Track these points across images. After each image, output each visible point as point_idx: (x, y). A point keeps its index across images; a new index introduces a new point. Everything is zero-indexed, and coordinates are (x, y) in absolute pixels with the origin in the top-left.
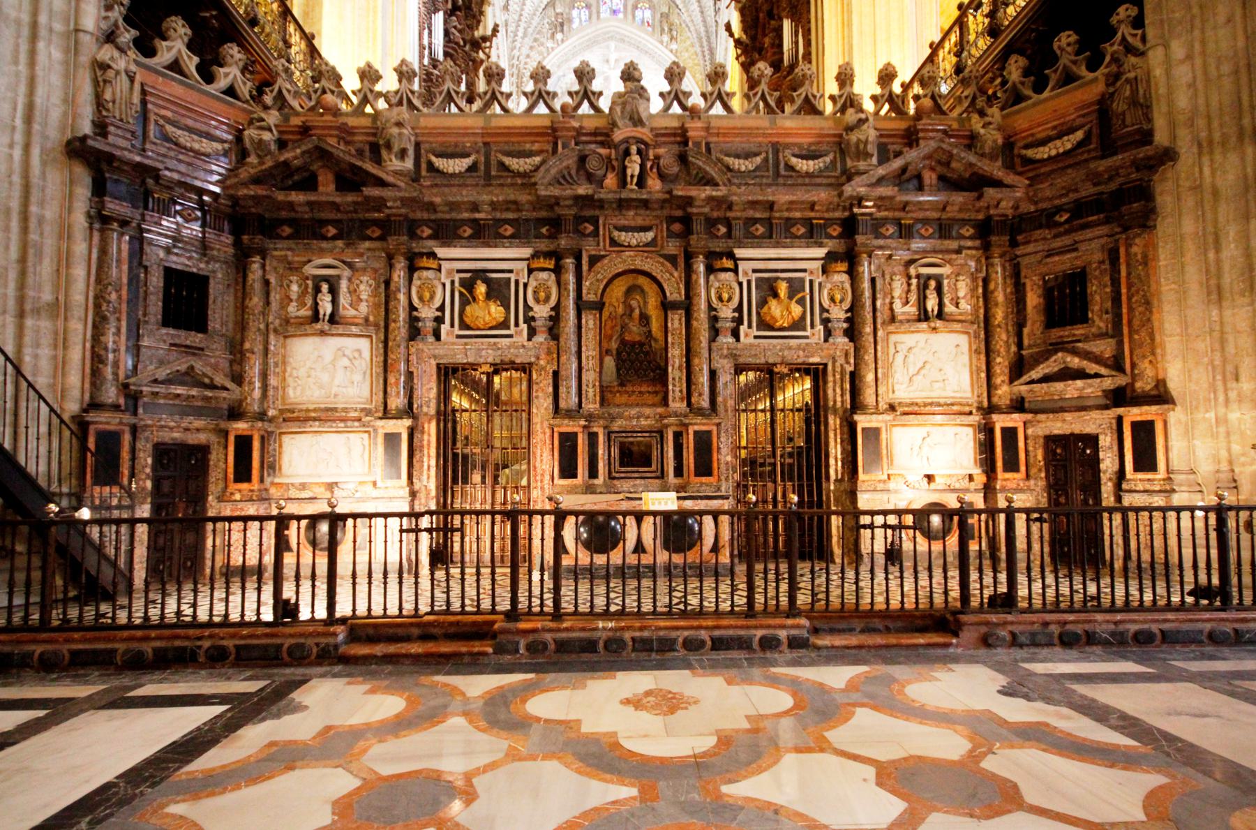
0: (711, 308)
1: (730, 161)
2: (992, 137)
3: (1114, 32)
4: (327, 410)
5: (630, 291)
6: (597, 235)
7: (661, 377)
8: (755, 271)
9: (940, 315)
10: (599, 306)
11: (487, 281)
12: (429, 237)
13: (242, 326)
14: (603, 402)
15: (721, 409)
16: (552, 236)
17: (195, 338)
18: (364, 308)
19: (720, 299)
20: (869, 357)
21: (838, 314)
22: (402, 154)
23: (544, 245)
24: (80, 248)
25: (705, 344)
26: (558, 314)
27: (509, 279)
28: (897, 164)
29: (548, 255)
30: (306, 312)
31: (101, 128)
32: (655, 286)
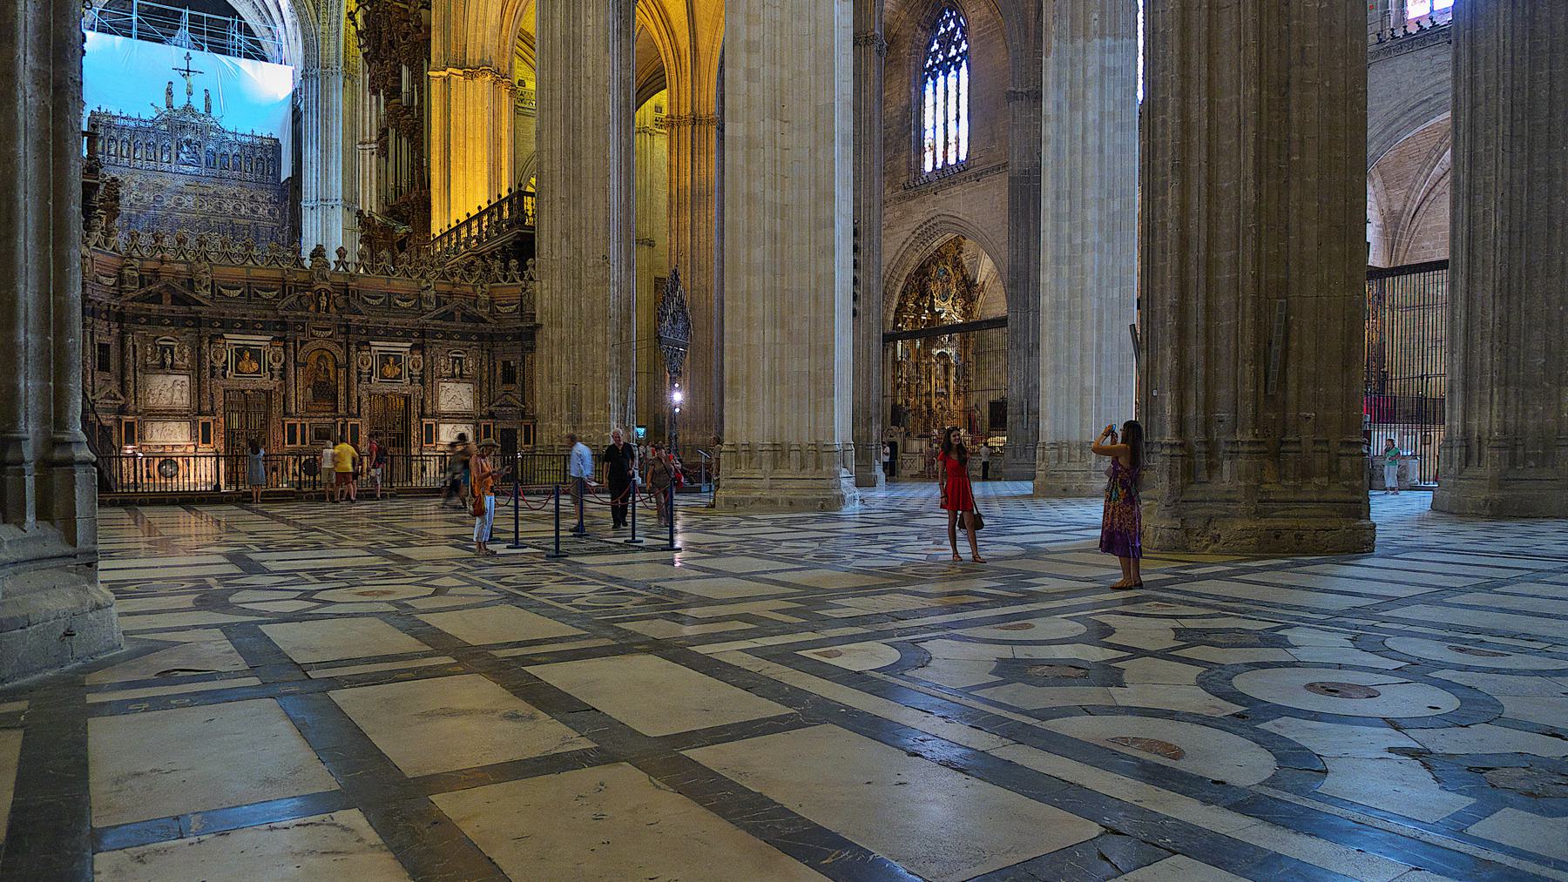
3: (526, 269)
4: (171, 411)
6: (304, 331)
8: (379, 351)
11: (249, 350)
12: (219, 327)
15: (362, 414)
16: (285, 330)
18: (186, 361)
19: (362, 363)
21: (416, 372)
22: (206, 287)
23: (277, 334)
25: (355, 385)
26: (285, 368)
27: (260, 350)
29: (280, 339)
32: (332, 357)
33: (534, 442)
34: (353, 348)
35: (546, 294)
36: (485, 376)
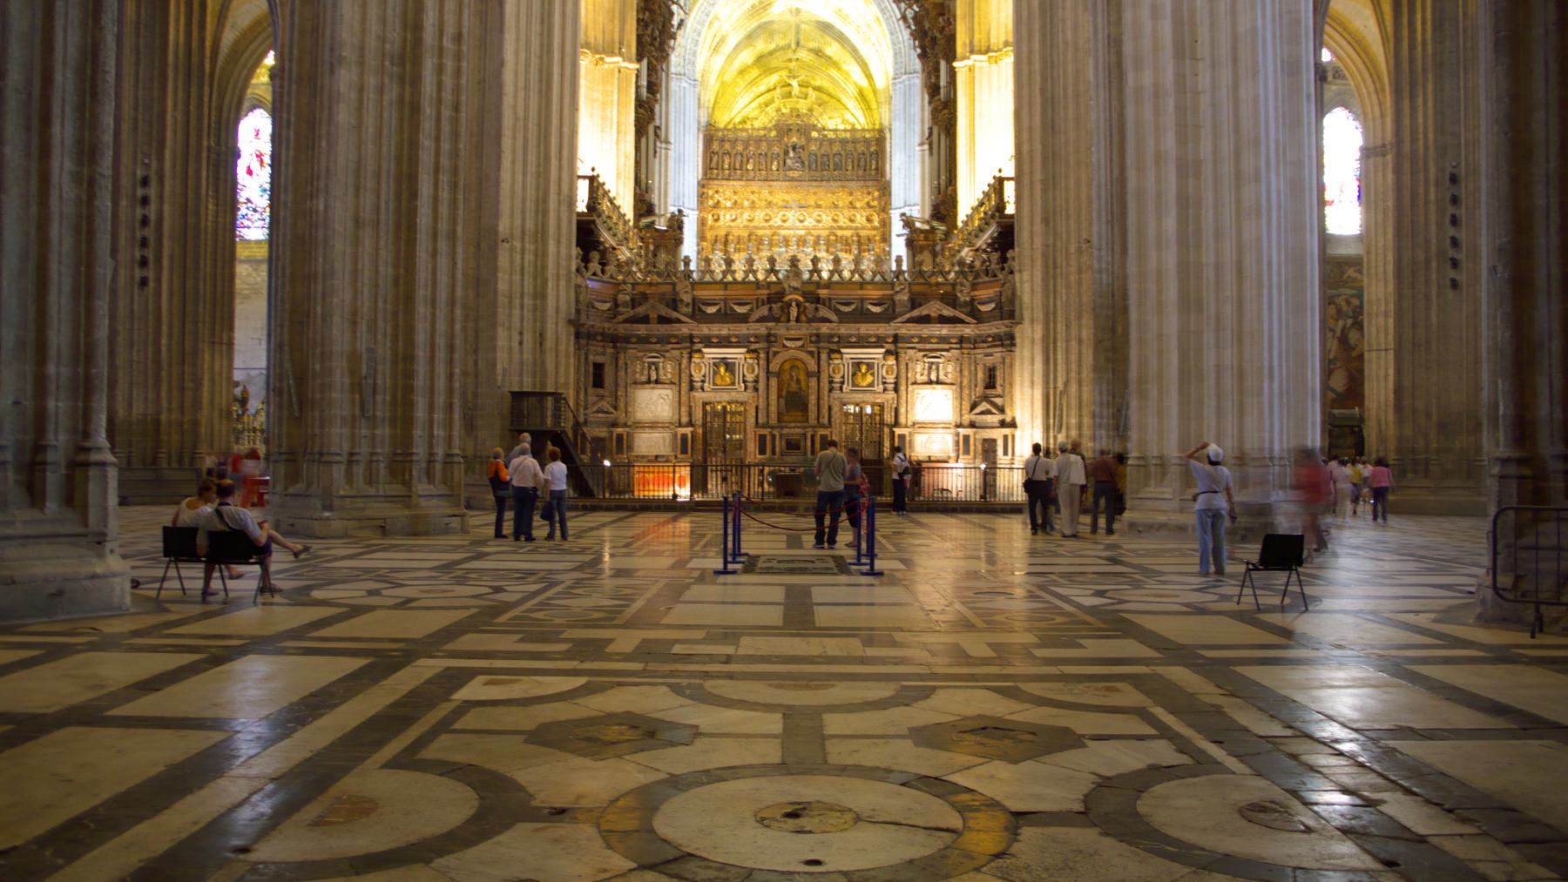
0: (830, 376)
1: (839, 307)
2: (963, 297)
5: (792, 367)
7: (805, 409)
9: (938, 382)
10: (778, 374)
13: (617, 385)
14: (779, 420)
17: (601, 391)
18: (669, 376)
20: (903, 401)
21: (891, 379)
23: (753, 347)
24: (572, 360)
25: (826, 393)
28: (916, 313)
29: (755, 351)
30: (644, 379)
31: (578, 311)
33: (1013, 454)
34: (824, 356)
35: (1027, 287)
36: (965, 382)
